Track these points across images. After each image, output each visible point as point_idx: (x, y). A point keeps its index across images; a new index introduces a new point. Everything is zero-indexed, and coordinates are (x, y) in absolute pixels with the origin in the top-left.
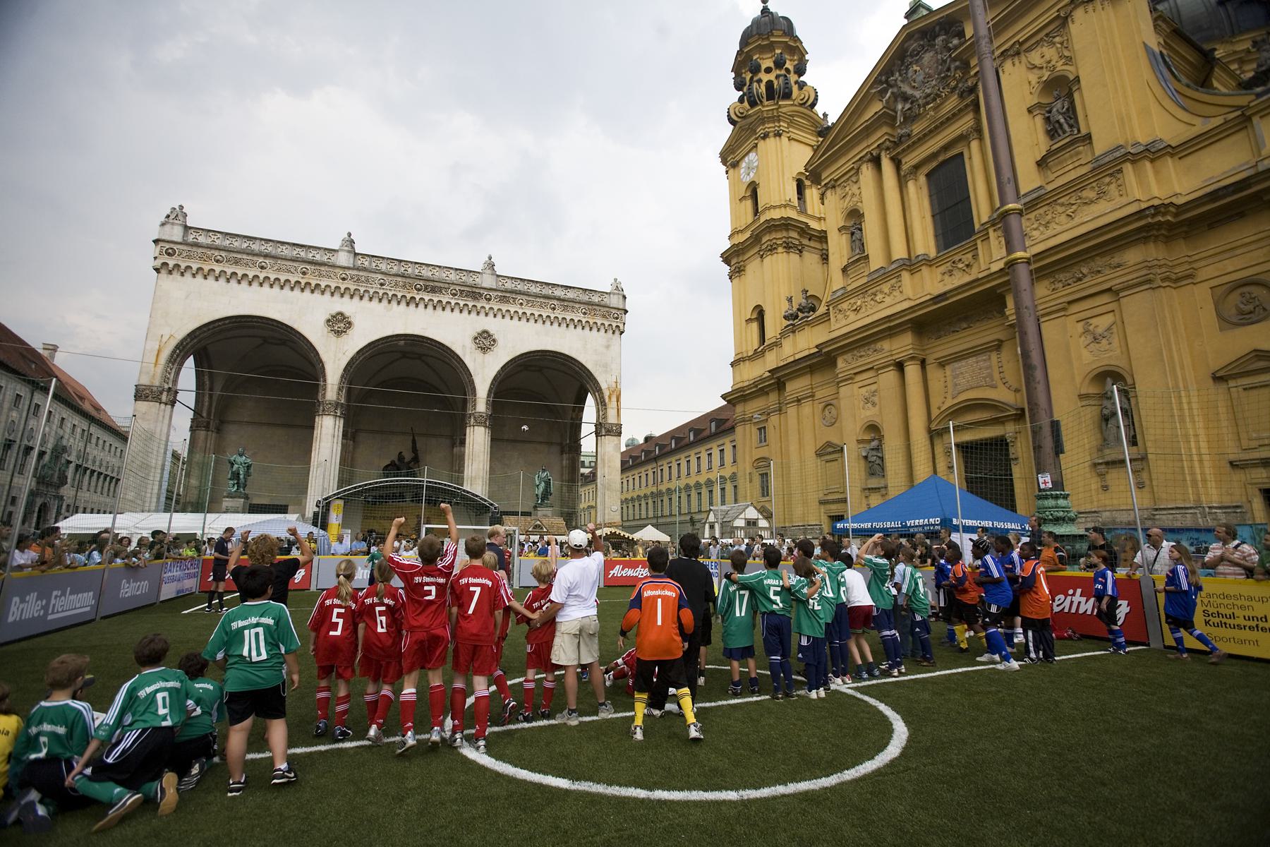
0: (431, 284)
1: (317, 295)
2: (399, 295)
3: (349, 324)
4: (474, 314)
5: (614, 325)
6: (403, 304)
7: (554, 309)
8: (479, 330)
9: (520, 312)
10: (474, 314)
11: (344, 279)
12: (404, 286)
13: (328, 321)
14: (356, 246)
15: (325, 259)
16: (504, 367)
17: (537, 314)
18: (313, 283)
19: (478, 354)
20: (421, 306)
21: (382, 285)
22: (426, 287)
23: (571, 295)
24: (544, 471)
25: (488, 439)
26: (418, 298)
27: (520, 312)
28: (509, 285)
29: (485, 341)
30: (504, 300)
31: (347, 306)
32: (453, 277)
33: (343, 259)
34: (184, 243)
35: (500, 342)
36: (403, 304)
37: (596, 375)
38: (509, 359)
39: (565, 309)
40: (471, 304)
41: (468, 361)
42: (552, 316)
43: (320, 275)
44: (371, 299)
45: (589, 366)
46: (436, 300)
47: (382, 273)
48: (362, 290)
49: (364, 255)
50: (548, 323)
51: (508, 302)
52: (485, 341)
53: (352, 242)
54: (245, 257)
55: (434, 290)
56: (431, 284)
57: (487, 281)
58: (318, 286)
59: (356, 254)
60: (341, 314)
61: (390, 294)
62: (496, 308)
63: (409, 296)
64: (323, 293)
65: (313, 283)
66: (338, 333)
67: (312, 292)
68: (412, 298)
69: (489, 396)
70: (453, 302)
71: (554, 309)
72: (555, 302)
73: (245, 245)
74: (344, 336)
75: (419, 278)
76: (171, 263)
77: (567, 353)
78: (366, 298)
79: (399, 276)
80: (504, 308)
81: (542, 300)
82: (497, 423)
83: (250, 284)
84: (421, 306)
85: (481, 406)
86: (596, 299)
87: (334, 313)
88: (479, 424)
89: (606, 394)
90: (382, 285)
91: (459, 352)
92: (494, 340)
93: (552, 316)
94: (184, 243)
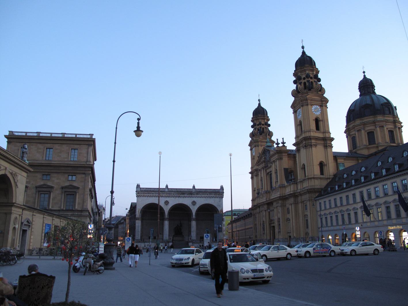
0: (183, 193)
1: (162, 198)
2: (177, 196)
3: (168, 203)
4: (191, 198)
5: (221, 196)
6: (178, 197)
7: (208, 195)
8: (193, 201)
9: (201, 196)
10: (191, 198)
11: (167, 194)
12: (178, 194)
13: (165, 202)
14: (168, 186)
15: (163, 190)
16: (198, 208)
17: (204, 196)
18: (162, 195)
19: (193, 206)
20: (181, 197)
21: (174, 194)
22: (182, 193)
23: (211, 191)
24: (207, 229)
25: (196, 223)
26: (180, 196)
27: (201, 196)
28: (198, 191)
29: (194, 203)
30: (197, 194)
31: (168, 199)
32: (187, 190)
33: (166, 190)
34: (141, 191)
35: (197, 203)
36: (178, 197)
37: (217, 208)
38: (199, 206)
39: (210, 194)
40: (191, 196)
41: (191, 208)
42: (207, 196)
43: (163, 194)
44: (172, 197)
45: (216, 206)
46: (184, 196)
47: (174, 192)
48: (170, 196)
49: (170, 189)
50: (207, 198)
51: (198, 194)
52: (194, 203)
53: (168, 186)
54: (150, 192)
55: (183, 194)
56: (183, 193)
57: (194, 191)
58: (162, 196)
59: (169, 189)
60: (167, 201)
61: (175, 196)
62: (196, 196)
63: (179, 196)
64: (163, 197)
65: (162, 195)
66: (167, 205)
67: (162, 197)
68: (179, 196)
69: (195, 214)
70: (187, 196)
71: (208, 195)
72: (208, 193)
73: (150, 190)
74: (168, 205)
75: (180, 192)
76: (139, 195)
77: (211, 203)
78: (171, 197)
79: (176, 192)
80: (197, 196)
81: (205, 193)
82: (197, 220)
83: (151, 197)
84: (181, 197)
85: (194, 217)
86: (217, 191)
87: (165, 201)
88: (194, 221)
89: (220, 212)
90: (174, 194)
91: (189, 206)
92: (196, 203)
93: (207, 196)
94: (141, 191)
